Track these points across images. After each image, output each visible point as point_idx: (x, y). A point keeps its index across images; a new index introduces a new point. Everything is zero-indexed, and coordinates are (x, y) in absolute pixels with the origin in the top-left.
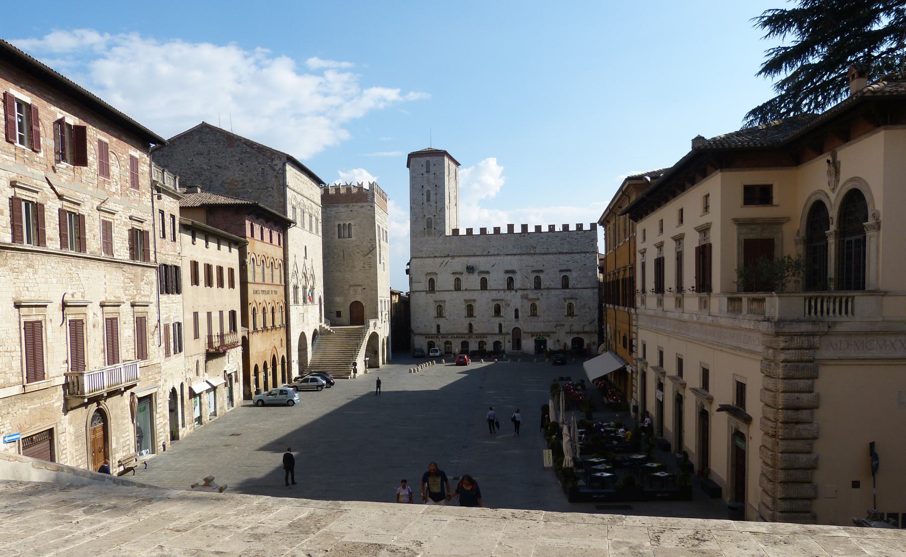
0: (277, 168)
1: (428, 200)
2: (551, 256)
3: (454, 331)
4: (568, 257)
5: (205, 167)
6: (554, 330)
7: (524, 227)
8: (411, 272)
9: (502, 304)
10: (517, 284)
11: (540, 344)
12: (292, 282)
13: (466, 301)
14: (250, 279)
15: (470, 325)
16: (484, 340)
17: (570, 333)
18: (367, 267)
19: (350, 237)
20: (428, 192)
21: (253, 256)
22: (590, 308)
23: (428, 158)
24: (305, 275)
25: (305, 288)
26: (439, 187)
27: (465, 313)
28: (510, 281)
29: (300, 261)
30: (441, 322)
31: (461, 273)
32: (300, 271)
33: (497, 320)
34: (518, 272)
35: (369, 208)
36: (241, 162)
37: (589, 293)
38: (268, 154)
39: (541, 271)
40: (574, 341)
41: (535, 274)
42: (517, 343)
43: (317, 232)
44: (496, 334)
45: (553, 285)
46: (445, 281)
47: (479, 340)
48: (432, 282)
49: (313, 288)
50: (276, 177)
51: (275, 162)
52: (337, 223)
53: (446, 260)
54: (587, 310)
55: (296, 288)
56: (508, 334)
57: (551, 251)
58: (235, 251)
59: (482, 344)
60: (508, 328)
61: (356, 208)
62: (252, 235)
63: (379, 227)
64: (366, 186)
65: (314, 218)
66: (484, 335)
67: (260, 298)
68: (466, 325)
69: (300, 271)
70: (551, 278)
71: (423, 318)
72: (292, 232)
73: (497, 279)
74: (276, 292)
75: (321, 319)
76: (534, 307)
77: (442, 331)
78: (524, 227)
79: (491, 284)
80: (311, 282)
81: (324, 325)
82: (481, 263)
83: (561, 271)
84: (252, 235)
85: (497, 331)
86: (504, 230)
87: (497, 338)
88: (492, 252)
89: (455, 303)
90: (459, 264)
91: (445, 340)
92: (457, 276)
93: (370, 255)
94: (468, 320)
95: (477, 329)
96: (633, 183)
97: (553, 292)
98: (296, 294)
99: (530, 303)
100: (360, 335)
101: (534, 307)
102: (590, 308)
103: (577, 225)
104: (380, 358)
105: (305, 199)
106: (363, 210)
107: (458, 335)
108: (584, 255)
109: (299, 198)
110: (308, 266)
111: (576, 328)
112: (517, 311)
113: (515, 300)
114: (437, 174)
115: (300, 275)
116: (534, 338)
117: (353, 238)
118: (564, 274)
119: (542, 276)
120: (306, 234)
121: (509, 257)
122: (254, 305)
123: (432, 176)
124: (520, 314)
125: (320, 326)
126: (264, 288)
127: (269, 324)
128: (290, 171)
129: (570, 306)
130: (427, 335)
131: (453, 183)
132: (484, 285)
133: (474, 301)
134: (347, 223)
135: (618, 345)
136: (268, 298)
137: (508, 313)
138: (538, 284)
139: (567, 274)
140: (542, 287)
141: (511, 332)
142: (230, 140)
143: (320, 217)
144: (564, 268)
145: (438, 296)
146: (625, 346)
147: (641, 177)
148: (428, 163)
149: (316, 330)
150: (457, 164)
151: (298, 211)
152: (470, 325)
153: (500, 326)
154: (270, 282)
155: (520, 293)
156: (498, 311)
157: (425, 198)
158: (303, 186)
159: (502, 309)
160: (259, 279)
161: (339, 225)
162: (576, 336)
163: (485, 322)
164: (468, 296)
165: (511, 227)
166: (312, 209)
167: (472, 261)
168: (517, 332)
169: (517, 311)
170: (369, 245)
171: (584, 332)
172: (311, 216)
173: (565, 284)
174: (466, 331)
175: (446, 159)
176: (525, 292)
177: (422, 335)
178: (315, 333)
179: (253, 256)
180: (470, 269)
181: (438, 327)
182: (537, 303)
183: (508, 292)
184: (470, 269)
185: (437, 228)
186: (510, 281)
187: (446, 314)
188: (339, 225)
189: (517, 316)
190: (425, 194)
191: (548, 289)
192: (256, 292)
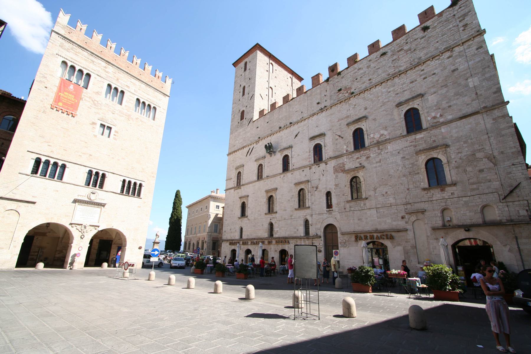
2: (378, 88)
4: (412, 75)
6: (401, 224)
10: (326, 153)
17: (446, 227)
22: (491, 159)
28: (318, 150)
33: (303, 214)
44: (300, 238)
54: (485, 164)
68: (266, 226)
73: (301, 154)
77: (244, 237)
79: (293, 162)
82: (281, 139)
83: (399, 105)
85: (301, 232)
88: (294, 120)
97: (390, 147)
99: (349, 177)
102: (491, 159)
107: (255, 241)
108: (448, 54)
111: (462, 214)
118: (405, 108)
119: (363, 125)
124: (334, 201)
137: (317, 201)
138: (359, 138)
139: (415, 104)
141: (321, 233)
152: (271, 225)
153: (307, 222)
159: (308, 196)
162: (461, 234)
168: (330, 229)
171: (486, 224)
173: (413, 121)
174: (266, 235)
176: (340, 160)
182: (360, 174)
183: (315, 168)
186: (318, 150)
187: (248, 212)
189: (329, 206)
191: (378, 143)
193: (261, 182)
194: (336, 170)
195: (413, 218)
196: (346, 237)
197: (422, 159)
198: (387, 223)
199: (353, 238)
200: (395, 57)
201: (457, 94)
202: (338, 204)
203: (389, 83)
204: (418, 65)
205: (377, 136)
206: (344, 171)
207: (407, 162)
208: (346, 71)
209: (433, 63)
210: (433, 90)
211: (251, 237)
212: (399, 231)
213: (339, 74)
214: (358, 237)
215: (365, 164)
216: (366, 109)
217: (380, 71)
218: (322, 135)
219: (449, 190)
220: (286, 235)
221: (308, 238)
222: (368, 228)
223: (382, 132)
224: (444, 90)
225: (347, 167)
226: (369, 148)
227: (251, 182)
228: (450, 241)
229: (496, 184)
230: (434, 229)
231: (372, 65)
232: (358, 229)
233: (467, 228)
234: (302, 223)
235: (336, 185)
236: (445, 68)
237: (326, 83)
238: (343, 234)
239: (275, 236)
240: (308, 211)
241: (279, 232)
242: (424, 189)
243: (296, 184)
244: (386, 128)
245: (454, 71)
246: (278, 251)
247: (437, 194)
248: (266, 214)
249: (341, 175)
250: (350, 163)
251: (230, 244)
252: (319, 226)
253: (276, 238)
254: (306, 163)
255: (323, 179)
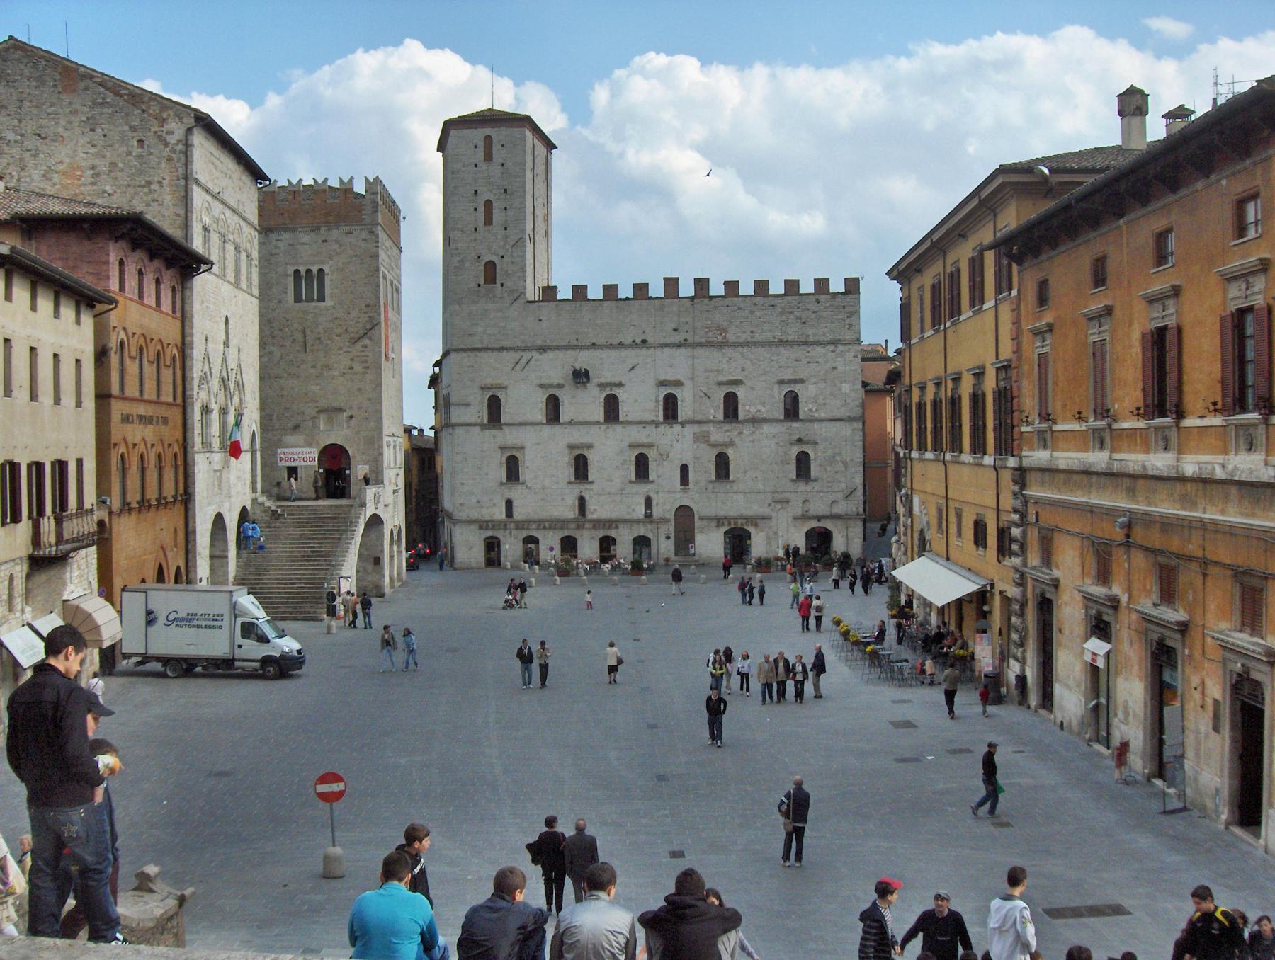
0: (172, 140)
1: (489, 221)
2: (759, 350)
3: (543, 515)
4: (798, 352)
5: (11, 136)
6: (765, 511)
7: (702, 284)
8: (445, 381)
9: (652, 454)
10: (684, 412)
11: (738, 542)
12: (199, 397)
13: (571, 447)
14: (115, 390)
15: (582, 502)
16: (613, 533)
17: (805, 517)
18: (358, 368)
19: (321, 298)
20: (488, 204)
21: (122, 335)
23: (488, 131)
24: (224, 381)
25: (224, 412)
26: (511, 191)
27: (569, 473)
29: (216, 350)
30: (517, 493)
31: (560, 386)
32: (216, 371)
33: (643, 489)
34: (688, 384)
35: (364, 234)
36: (91, 125)
37: (846, 430)
38: (154, 109)
39: (738, 383)
40: (810, 535)
41: (726, 390)
42: (684, 539)
43: (250, 285)
44: (638, 521)
45: (764, 412)
46: (524, 402)
47: (602, 533)
48: (494, 405)
49: (239, 415)
50: (170, 160)
51: (167, 127)
52: (291, 270)
53: (527, 355)
54: (840, 467)
55: (206, 410)
56: (666, 521)
57: (758, 338)
58: (88, 321)
59: (607, 544)
60: (665, 507)
61: (335, 234)
62: (122, 288)
63: (385, 278)
64: (360, 188)
65: (243, 256)
66: (612, 523)
67: (137, 433)
68: (572, 501)
69: (216, 371)
70: (759, 398)
71: (470, 489)
72: (202, 283)
73: (640, 401)
74: (166, 421)
75: (254, 482)
76: (722, 464)
77: (518, 514)
78: (702, 284)
79: (625, 411)
80: (236, 400)
81: (262, 499)
82: (606, 367)
83: (781, 382)
84: (122, 288)
85: (640, 511)
86: (657, 290)
87: (641, 531)
89: (546, 455)
90: (555, 368)
91: (525, 534)
92: (551, 391)
93: (366, 341)
94: (577, 489)
95: (597, 510)
96: (1012, 181)
97: (766, 428)
98: (206, 425)
99: (714, 452)
100: (342, 525)
101: (722, 464)
102: (845, 464)
103: (817, 281)
104: (387, 573)
105: (228, 213)
106: (351, 239)
108: (831, 348)
109: (217, 208)
110: (232, 364)
111: (819, 507)
112: (684, 469)
113: (678, 445)
114: (509, 164)
115: (215, 383)
116: (725, 529)
117: (329, 302)
118: (787, 388)
119: (741, 392)
120: (226, 289)
121: (667, 351)
122: (122, 449)
123: (497, 170)
125: (254, 501)
126: (142, 410)
127: (152, 495)
128: (199, 140)
129: (803, 463)
130: (483, 524)
131: (540, 186)
132: (612, 409)
133: (590, 446)
134: (315, 269)
135: (954, 541)
136: (149, 432)
137: (664, 474)
139: (797, 388)
140: (741, 417)
141: (671, 515)
142: (69, 75)
143: (255, 254)
144: (788, 375)
145: (509, 437)
146: (980, 538)
147: (1027, 168)
148: (488, 139)
149: (244, 509)
150: (551, 146)
151: (214, 237)
152: (582, 502)
153: (648, 502)
154: (154, 397)
155: (689, 431)
156: (642, 467)
157: (481, 215)
158: (224, 182)
159: (652, 466)
160: (132, 390)
161: (297, 272)
162: (814, 524)
163: (614, 496)
164: (579, 436)
165: (671, 284)
166: (241, 233)
167: (583, 360)
168: (684, 514)
169: (684, 469)
170: (364, 318)
172: (237, 249)
174: (571, 513)
175: (529, 134)
176: (705, 428)
177: (470, 522)
178: (244, 516)
179: (122, 335)
180: (581, 377)
181: (509, 504)
182: (730, 452)
183: (664, 429)
184: (581, 377)
185: (508, 284)
187: (525, 474)
188: (297, 272)
189: (684, 480)
190: (481, 209)
191: (754, 421)
192: (126, 419)
193: (557, 429)
194: (696, 438)
195: (779, 506)
196: (705, 522)
197: (795, 450)
198: (755, 509)
199: (714, 524)
200: (784, 318)
201: (832, 394)
202: (697, 483)
203: (774, 349)
204: (806, 343)
205: (753, 410)
206: (707, 442)
207: (781, 450)
208: (721, 302)
209: (819, 350)
210: (814, 380)
211: (536, 517)
212: (764, 518)
213: (711, 298)
214: (719, 521)
215: (737, 440)
216: (743, 370)
217: (766, 326)
218: (678, 384)
219: (812, 484)
220: (614, 516)
221: (651, 522)
222: (732, 513)
223: (759, 407)
224: (822, 385)
225: (713, 439)
226: (742, 422)
227: (532, 424)
228: (806, 528)
229: (843, 485)
230: (795, 518)
231: (757, 313)
232: (722, 513)
233: (819, 519)
234: (643, 502)
235: (696, 458)
236: (827, 361)
237: (688, 303)
238: (702, 519)
239: (589, 516)
240: (650, 487)
241: (597, 510)
242: (792, 481)
243: (632, 446)
244: (763, 404)
245: (834, 368)
246: (598, 539)
247: (802, 487)
248: (570, 483)
249: (703, 446)
250: (717, 435)
251: (481, 528)
252: (668, 507)
253: (591, 521)
254: (649, 416)
255: (678, 446)
